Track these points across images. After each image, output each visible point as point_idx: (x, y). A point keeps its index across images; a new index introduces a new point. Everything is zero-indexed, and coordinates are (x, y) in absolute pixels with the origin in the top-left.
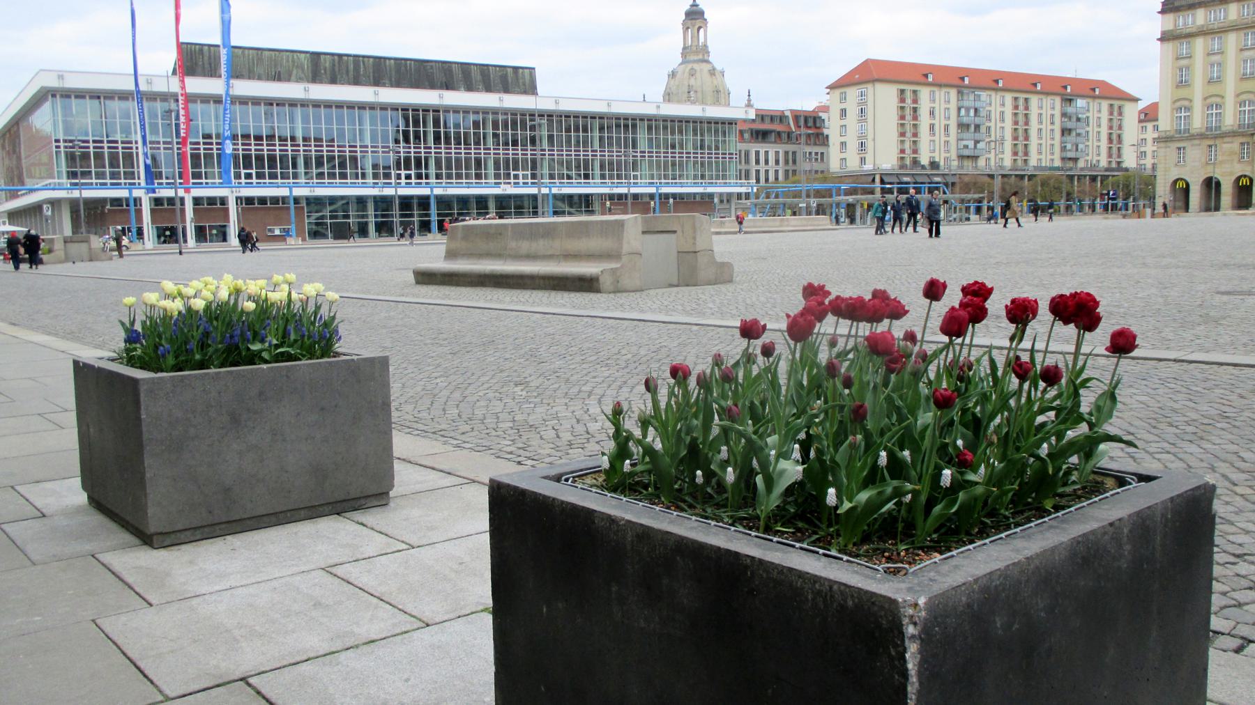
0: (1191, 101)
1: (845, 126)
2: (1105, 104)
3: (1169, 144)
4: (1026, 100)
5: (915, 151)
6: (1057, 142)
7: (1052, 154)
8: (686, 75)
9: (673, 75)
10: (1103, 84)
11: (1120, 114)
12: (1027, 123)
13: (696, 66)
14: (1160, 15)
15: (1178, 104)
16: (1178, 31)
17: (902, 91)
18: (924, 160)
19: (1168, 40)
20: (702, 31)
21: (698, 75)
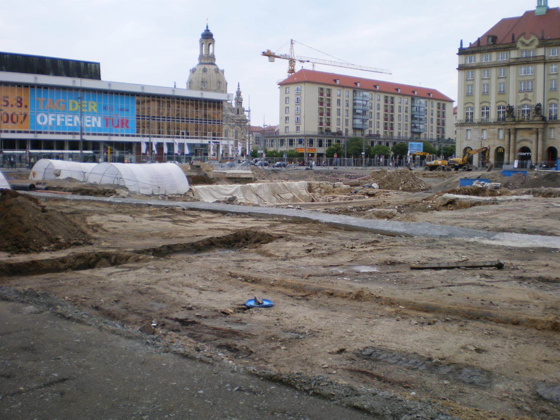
0: (474, 104)
1: (288, 107)
2: (435, 103)
3: (462, 127)
4: (392, 98)
5: (329, 124)
6: (409, 123)
7: (406, 129)
8: (201, 72)
9: (193, 71)
10: (434, 92)
11: (444, 109)
12: (392, 111)
13: (207, 67)
14: (458, 55)
15: (467, 106)
16: (467, 65)
17: (322, 89)
18: (334, 129)
19: (462, 69)
20: (211, 46)
21: (208, 72)
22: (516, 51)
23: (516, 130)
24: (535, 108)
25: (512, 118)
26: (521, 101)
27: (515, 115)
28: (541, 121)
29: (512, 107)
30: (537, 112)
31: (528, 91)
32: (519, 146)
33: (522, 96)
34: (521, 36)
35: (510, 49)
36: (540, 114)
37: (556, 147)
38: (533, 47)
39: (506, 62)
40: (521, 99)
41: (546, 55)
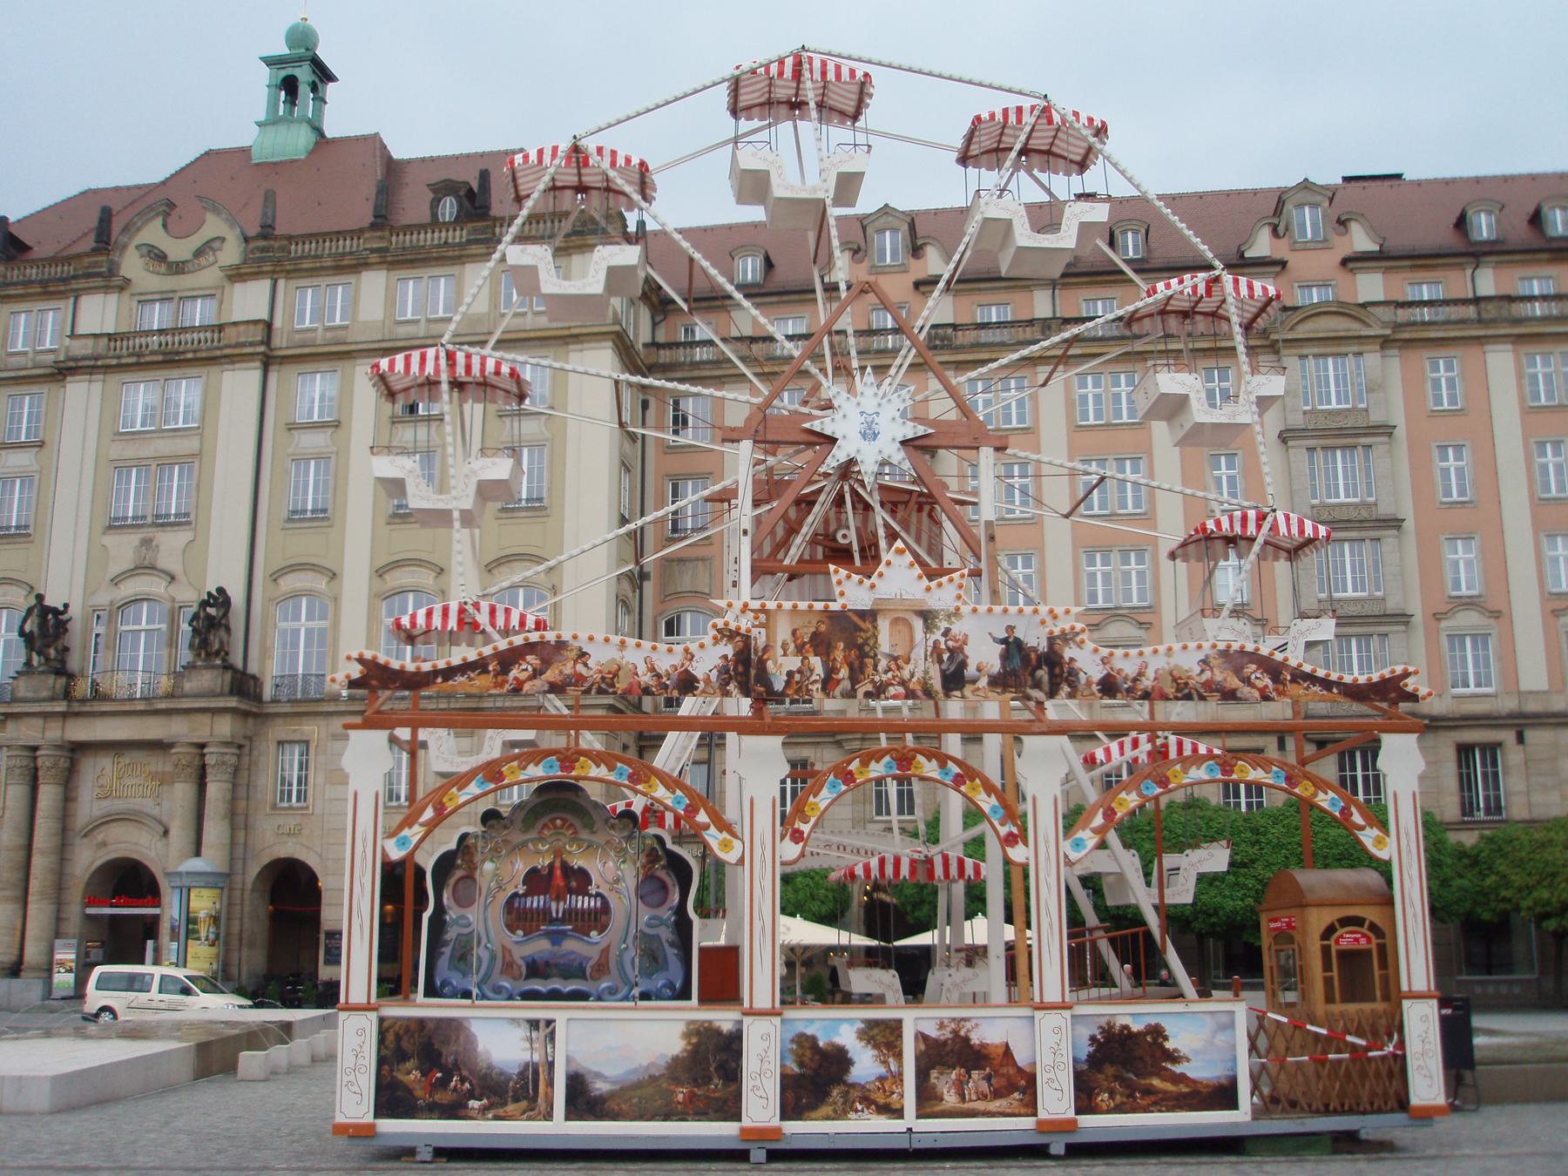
22: (113, 298)
23: (78, 750)
24: (196, 617)
25: (51, 679)
26: (116, 581)
27: (73, 664)
28: (221, 695)
29: (56, 612)
30: (205, 644)
31: (162, 523)
32: (86, 860)
33: (124, 549)
34: (146, 215)
35: (75, 285)
36: (223, 652)
37: (312, 861)
38: (209, 276)
39: (51, 358)
40: (115, 569)
41: (278, 323)
